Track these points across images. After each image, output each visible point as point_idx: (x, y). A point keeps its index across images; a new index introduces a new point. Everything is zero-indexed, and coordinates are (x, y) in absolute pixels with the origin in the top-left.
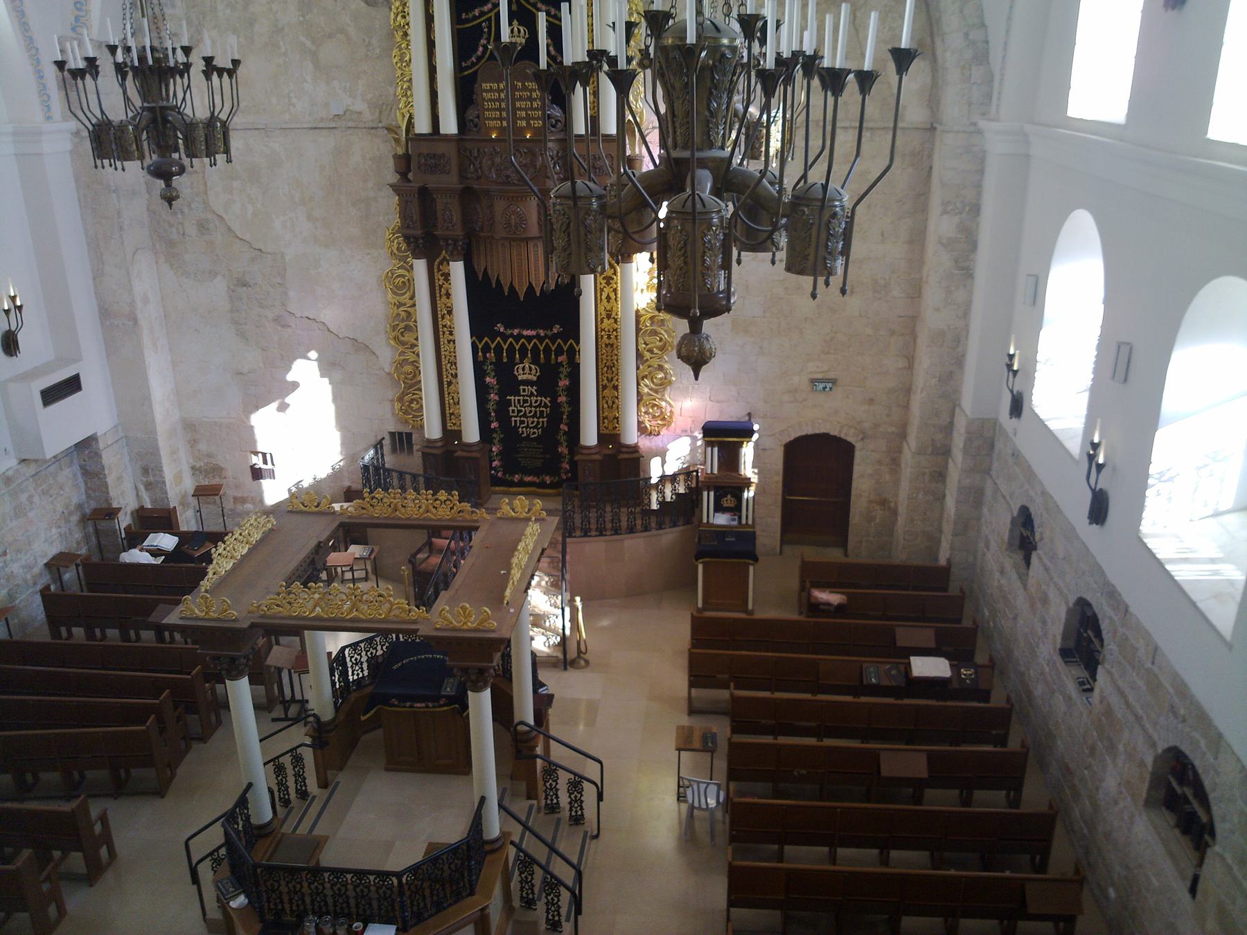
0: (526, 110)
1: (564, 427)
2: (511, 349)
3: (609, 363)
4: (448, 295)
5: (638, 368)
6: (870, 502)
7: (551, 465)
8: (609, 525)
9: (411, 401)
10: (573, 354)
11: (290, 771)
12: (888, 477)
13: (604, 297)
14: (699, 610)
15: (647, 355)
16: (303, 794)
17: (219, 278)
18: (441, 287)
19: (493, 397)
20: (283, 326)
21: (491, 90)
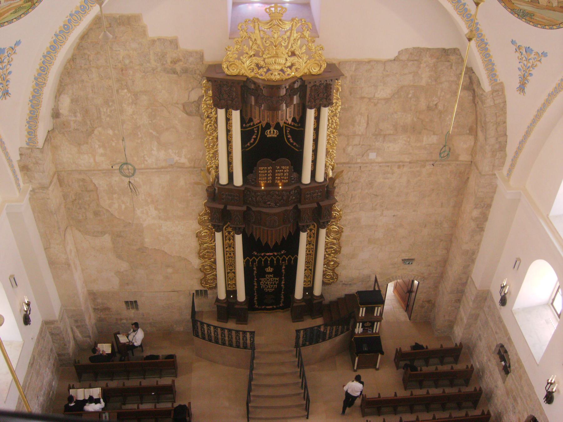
0: (280, 176)
6: (423, 302)
12: (433, 292)
17: (107, 235)
18: (226, 236)
21: (263, 170)
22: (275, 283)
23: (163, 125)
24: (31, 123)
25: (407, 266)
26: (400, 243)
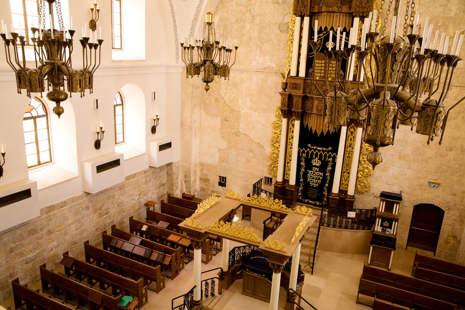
2: (312, 153)
3: (348, 164)
4: (293, 132)
5: (358, 167)
6: (449, 236)
7: (320, 198)
8: (338, 224)
9: (274, 167)
10: (334, 158)
11: (210, 286)
12: (458, 227)
13: (349, 138)
14: (368, 264)
15: (363, 162)
16: (213, 295)
17: (219, 117)
18: (291, 129)
19: (303, 170)
20: (237, 136)
22: (319, 178)
23: (265, 38)
24: (194, 22)
25: (432, 190)
26: (427, 163)
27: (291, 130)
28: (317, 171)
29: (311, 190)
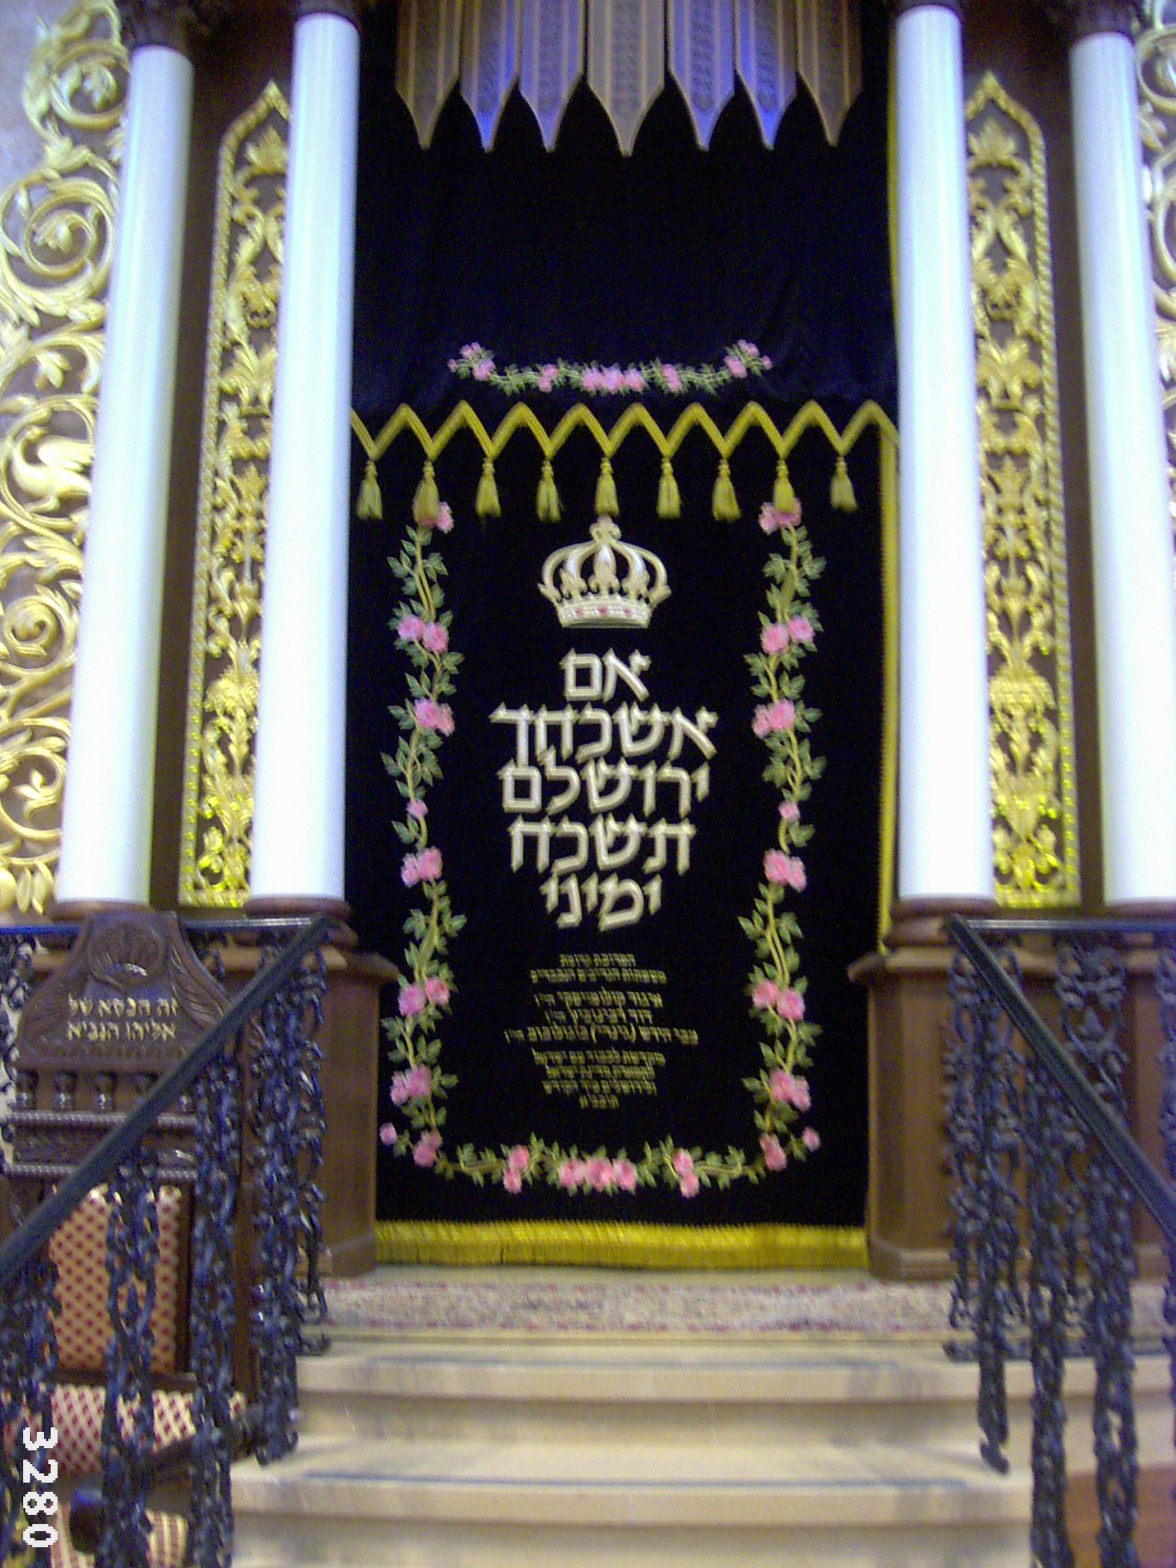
1: (785, 870)
4: (265, 262)
7: (705, 1096)
19: (428, 717)
22: (668, 791)
27: (247, 249)
28: (623, 695)
29: (574, 986)
